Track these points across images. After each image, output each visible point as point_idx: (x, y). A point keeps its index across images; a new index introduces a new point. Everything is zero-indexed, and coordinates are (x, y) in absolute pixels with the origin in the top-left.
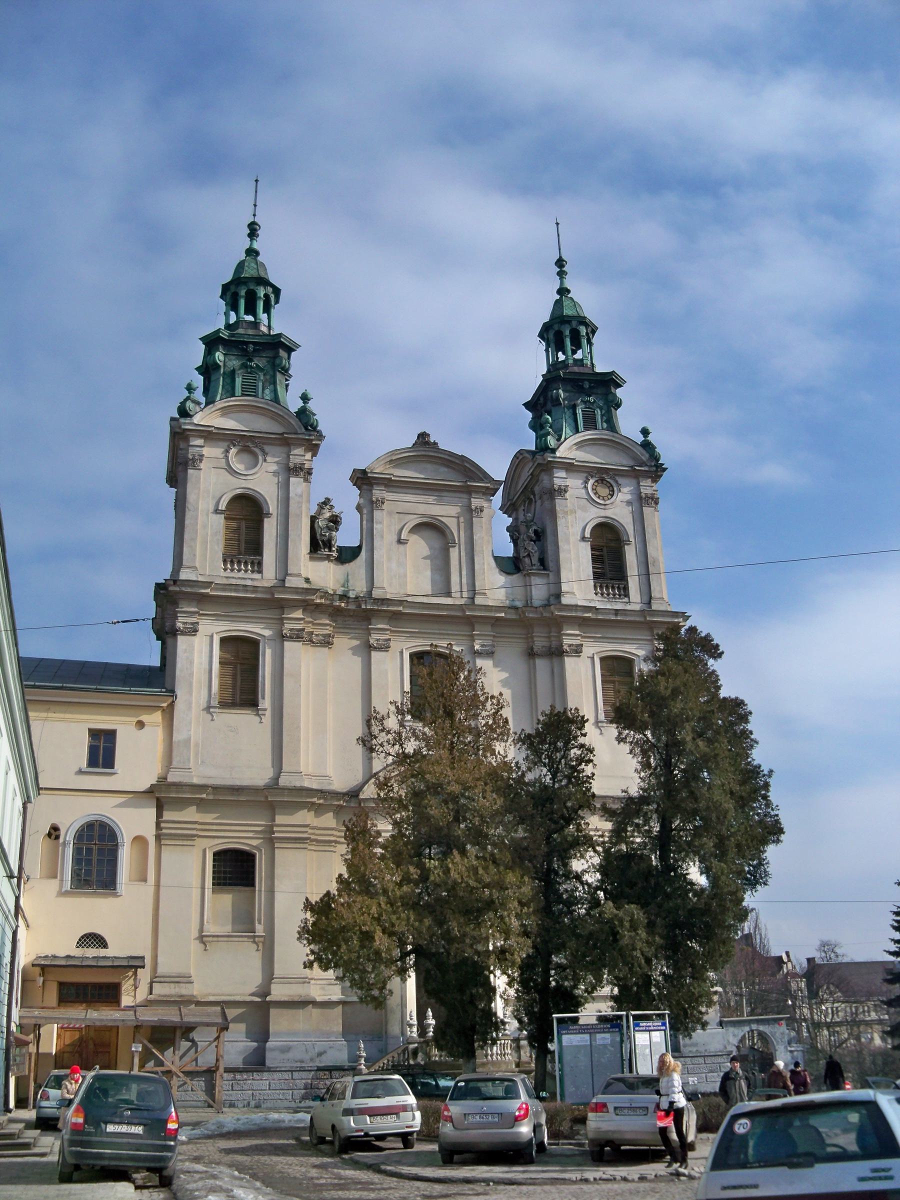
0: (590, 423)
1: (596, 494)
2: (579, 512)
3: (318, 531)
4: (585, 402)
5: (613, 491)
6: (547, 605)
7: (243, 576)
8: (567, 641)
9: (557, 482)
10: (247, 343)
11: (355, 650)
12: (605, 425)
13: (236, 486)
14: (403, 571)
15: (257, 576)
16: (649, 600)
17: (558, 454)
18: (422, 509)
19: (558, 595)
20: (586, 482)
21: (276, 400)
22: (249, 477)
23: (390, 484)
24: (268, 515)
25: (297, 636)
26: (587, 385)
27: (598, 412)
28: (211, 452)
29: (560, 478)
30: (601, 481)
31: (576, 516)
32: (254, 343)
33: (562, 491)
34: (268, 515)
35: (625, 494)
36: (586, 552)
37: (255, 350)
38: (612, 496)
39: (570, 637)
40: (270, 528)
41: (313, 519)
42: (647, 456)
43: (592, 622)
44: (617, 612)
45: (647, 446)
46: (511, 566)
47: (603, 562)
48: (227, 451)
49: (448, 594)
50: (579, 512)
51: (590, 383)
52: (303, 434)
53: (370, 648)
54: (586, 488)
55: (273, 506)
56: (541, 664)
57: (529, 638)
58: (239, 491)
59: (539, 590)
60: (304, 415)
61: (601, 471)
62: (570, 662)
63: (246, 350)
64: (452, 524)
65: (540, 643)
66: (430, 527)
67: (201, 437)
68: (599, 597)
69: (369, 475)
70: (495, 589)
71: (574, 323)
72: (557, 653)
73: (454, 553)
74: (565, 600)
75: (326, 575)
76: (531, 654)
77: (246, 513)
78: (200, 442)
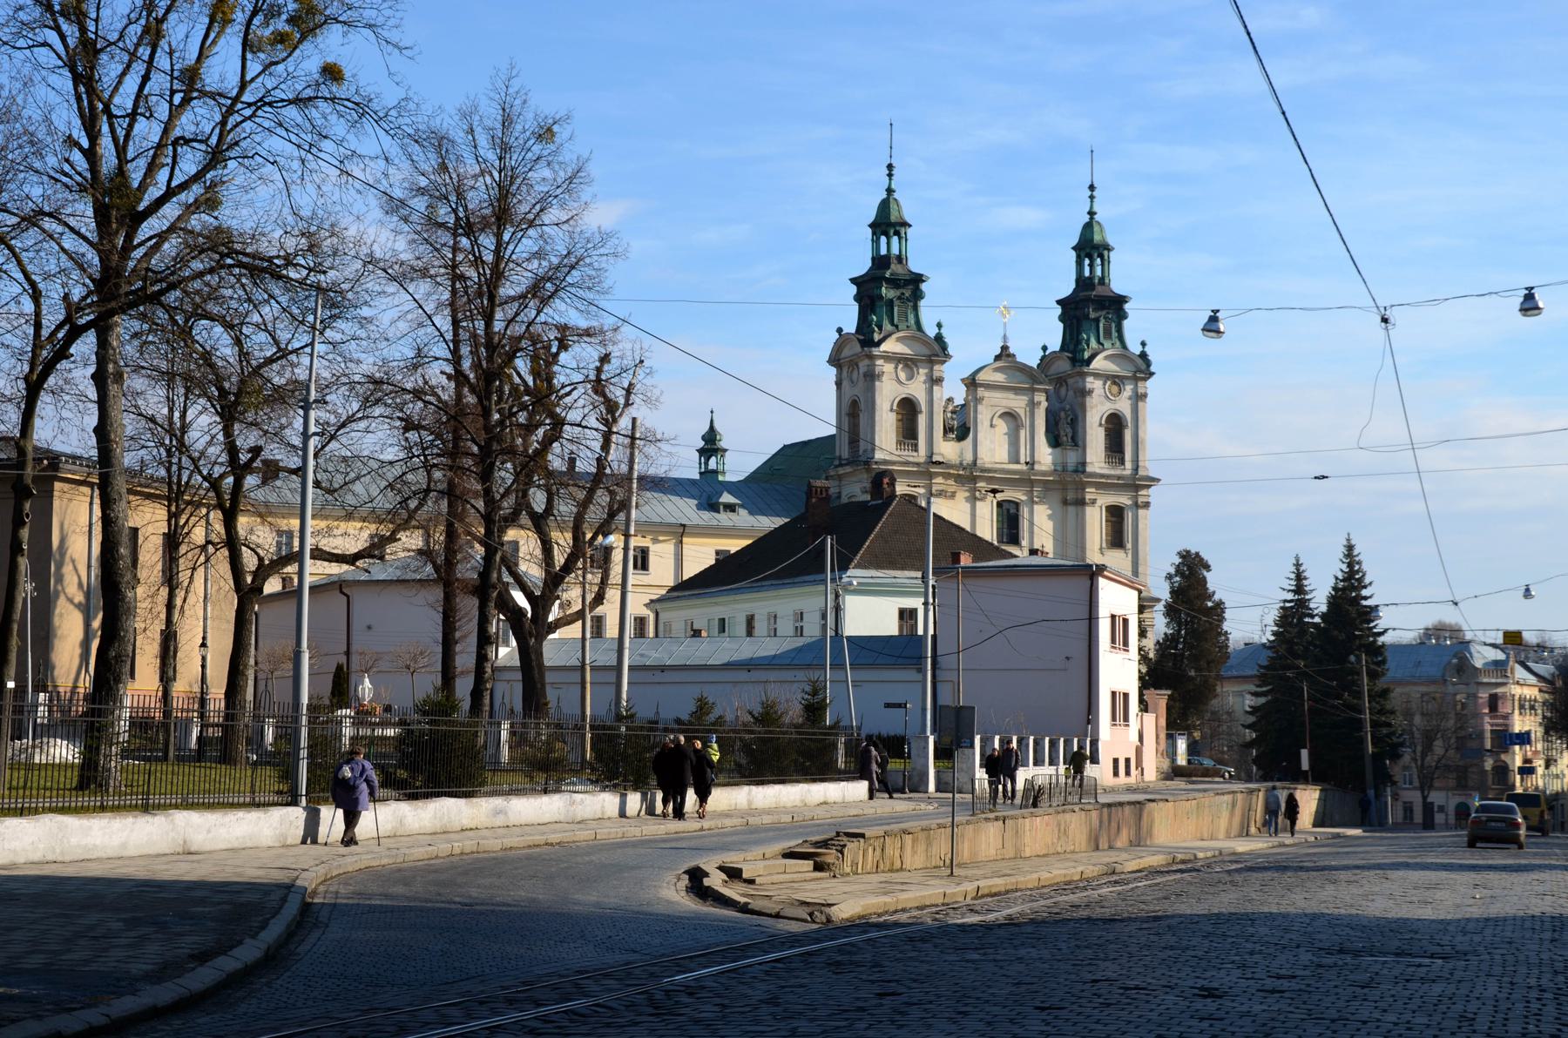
0: (1108, 335)
6: (1076, 471)
7: (909, 455)
8: (1088, 497)
9: (1088, 386)
11: (967, 499)
13: (903, 392)
14: (992, 447)
16: (1136, 469)
18: (1005, 403)
19: (1084, 464)
21: (918, 323)
25: (941, 494)
28: (888, 368)
29: (1093, 384)
30: (1114, 383)
31: (1097, 410)
33: (1091, 392)
35: (1128, 389)
39: (1090, 493)
40: (922, 420)
43: (1105, 485)
44: (1119, 478)
45: (1143, 356)
46: (1055, 441)
49: (1018, 462)
53: (976, 498)
55: (924, 407)
56: (1071, 509)
59: (1072, 458)
60: (939, 338)
62: (1088, 510)
64: (1021, 412)
65: (1070, 496)
66: (1010, 415)
70: (1045, 456)
72: (1081, 503)
73: (1022, 433)
74: (1089, 469)
75: (948, 450)
76: (1065, 502)
77: (908, 409)
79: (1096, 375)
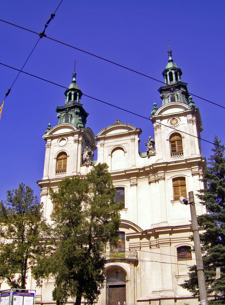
1: (171, 124)
2: (166, 132)
3: (84, 158)
4: (171, 95)
5: (178, 121)
10: (66, 108)
12: (179, 100)
15: (65, 174)
17: (155, 115)
20: (168, 121)
22: (63, 147)
23: (105, 139)
24: (69, 156)
26: (172, 89)
27: (176, 97)
32: (68, 108)
34: (69, 156)
36: (168, 145)
37: (69, 110)
38: (177, 123)
41: (82, 155)
42: (188, 106)
44: (176, 162)
47: (175, 146)
48: (58, 141)
50: (166, 132)
51: (173, 88)
52: (76, 130)
54: (168, 123)
57: (149, 178)
58: (60, 151)
61: (172, 116)
63: (66, 110)
66: (119, 148)
67: (50, 139)
68: (172, 158)
69: (98, 137)
71: (170, 70)
78: (50, 140)
79: (162, 118)
